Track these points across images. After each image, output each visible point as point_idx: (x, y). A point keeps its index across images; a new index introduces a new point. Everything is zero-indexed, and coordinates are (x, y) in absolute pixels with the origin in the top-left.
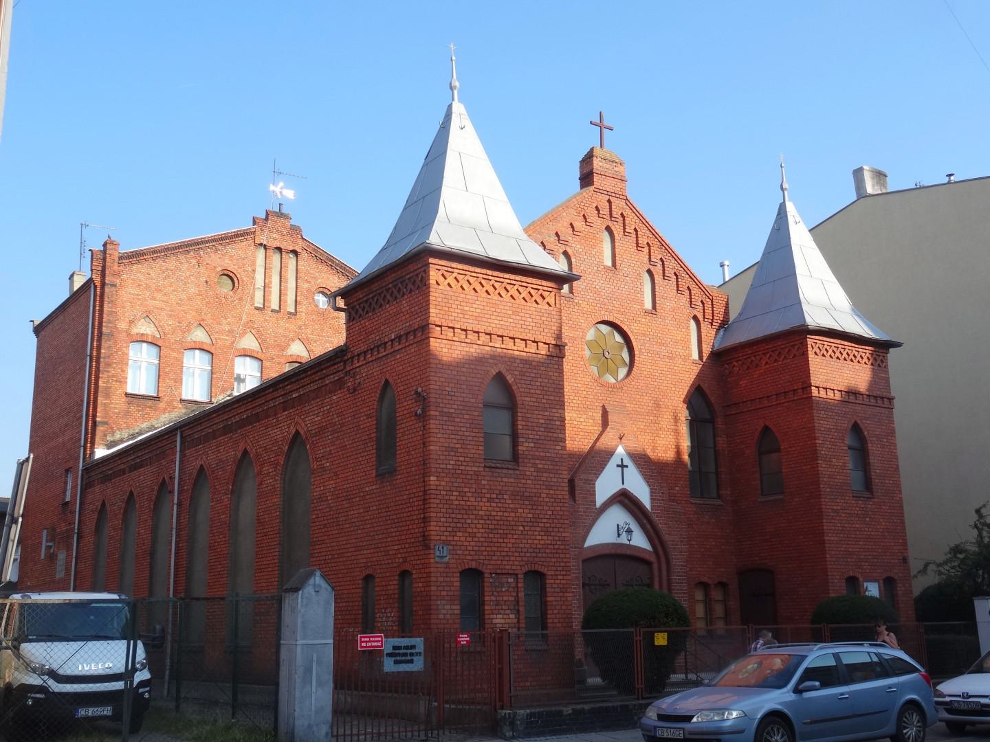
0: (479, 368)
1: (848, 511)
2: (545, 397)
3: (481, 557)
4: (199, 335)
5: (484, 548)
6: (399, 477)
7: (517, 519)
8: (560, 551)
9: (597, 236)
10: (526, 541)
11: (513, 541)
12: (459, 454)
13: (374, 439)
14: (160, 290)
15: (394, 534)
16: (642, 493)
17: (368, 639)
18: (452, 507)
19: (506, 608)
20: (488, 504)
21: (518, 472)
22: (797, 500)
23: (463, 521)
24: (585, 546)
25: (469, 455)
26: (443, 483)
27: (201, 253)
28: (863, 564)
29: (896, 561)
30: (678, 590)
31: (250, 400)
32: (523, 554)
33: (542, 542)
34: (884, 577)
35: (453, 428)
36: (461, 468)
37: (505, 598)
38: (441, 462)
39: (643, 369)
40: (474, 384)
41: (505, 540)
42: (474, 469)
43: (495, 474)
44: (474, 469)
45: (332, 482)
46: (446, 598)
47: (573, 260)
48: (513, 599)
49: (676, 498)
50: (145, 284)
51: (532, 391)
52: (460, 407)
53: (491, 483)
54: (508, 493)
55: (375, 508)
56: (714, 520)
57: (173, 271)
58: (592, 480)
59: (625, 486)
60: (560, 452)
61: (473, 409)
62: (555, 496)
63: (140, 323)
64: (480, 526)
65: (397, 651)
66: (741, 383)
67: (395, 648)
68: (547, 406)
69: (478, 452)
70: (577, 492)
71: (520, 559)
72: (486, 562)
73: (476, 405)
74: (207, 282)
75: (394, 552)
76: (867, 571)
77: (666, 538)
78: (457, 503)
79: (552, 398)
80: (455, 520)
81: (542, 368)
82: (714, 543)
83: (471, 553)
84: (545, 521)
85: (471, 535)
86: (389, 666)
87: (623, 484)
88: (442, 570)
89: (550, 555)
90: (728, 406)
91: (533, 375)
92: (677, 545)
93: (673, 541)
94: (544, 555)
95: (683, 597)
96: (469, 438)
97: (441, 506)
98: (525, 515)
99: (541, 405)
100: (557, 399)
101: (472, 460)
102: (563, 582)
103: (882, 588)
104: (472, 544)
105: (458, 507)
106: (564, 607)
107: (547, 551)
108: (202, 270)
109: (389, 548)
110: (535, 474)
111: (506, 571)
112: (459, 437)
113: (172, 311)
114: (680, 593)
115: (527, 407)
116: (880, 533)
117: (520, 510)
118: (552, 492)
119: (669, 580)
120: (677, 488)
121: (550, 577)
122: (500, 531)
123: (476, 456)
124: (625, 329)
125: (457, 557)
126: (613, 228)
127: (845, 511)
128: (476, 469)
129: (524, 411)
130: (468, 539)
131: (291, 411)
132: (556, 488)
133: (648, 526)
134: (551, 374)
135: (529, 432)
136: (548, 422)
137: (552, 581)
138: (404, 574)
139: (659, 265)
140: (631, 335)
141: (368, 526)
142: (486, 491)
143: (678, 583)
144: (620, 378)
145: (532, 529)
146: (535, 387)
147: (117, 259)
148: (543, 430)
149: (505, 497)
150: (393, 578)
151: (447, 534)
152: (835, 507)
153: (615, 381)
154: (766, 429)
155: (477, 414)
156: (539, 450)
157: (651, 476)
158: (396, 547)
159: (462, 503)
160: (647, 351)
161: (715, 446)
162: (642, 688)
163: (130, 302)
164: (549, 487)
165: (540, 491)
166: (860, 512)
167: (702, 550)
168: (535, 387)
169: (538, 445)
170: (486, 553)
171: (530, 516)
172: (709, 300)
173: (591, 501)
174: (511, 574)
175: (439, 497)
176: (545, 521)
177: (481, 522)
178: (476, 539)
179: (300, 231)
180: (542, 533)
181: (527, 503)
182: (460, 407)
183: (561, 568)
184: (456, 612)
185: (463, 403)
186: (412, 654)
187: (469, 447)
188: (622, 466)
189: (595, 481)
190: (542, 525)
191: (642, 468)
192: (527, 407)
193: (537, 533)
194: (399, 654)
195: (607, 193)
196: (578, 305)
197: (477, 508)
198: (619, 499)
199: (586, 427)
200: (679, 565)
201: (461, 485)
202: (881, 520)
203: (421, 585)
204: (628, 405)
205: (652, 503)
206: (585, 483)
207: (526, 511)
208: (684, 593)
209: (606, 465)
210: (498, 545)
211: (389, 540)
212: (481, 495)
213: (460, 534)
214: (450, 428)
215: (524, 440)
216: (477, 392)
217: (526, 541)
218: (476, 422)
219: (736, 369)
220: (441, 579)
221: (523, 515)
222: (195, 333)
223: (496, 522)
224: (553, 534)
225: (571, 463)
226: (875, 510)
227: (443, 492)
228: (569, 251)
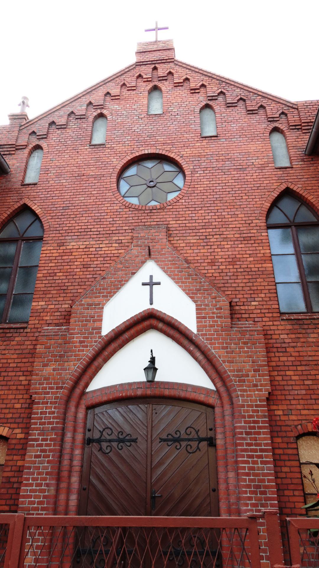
9: (141, 95)
30: (250, 445)
39: (196, 186)
49: (251, 316)
58: (99, 304)
77: (225, 367)
87: (151, 304)
92: (247, 376)
93: (238, 371)
95: (260, 457)
114: (256, 450)
120: (253, 303)
124: (172, 156)
133: (198, 354)
143: (247, 433)
157: (199, 290)
160: (202, 169)
167: (309, 382)
188: (151, 284)
191: (182, 282)
195: (152, 62)
200: (248, 406)
205: (198, 322)
206: (84, 309)
208: (262, 450)
228: (105, 112)
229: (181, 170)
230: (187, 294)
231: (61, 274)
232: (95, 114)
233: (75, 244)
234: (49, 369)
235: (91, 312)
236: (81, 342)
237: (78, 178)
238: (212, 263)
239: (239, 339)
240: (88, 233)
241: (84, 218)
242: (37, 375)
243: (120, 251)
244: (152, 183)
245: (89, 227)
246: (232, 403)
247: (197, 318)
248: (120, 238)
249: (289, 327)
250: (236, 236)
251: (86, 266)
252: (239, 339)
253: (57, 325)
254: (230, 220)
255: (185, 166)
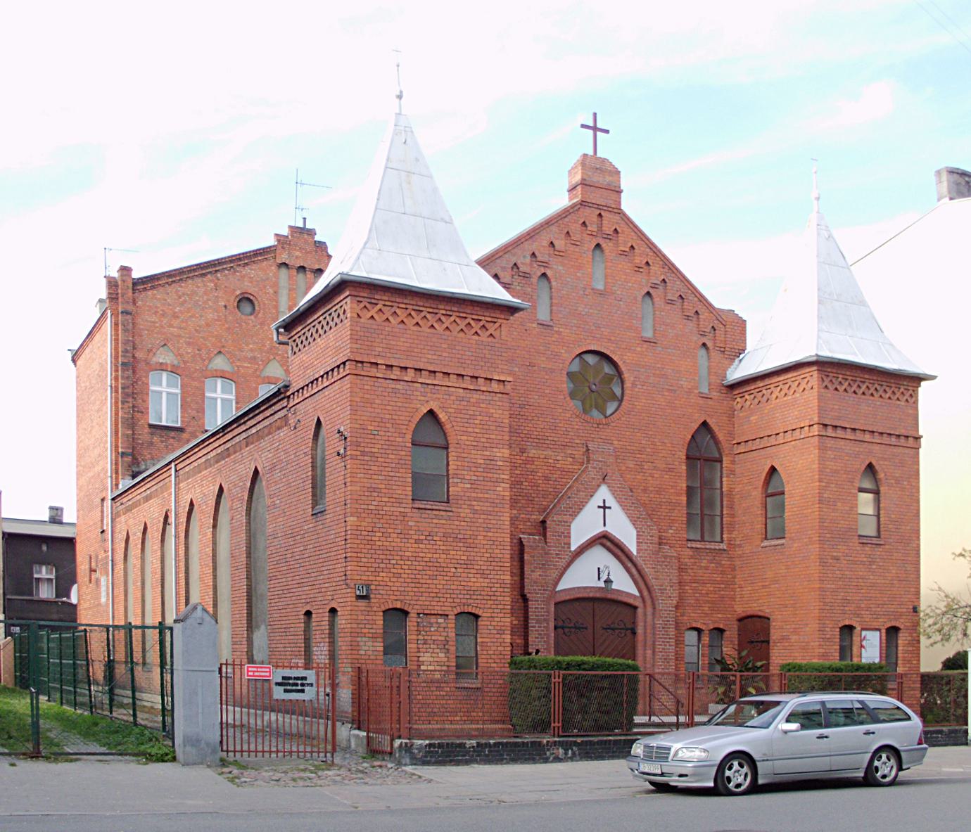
0: (407, 405)
1: (851, 558)
2: (485, 436)
3: (407, 597)
4: (220, 363)
5: (410, 589)
6: (328, 516)
7: (448, 561)
8: (499, 594)
10: (458, 583)
11: (444, 582)
12: (383, 495)
13: (310, 477)
14: (178, 317)
15: (325, 572)
16: (627, 535)
17: (255, 669)
18: (374, 547)
19: (435, 646)
20: (416, 545)
21: (451, 514)
22: (796, 545)
23: (387, 561)
24: (557, 590)
25: (394, 496)
26: (365, 524)
27: (219, 275)
28: (863, 612)
29: (905, 610)
31: (221, 435)
32: (455, 596)
33: (476, 584)
34: (889, 625)
35: (376, 468)
36: (385, 508)
37: (433, 638)
38: (362, 502)
39: (636, 403)
40: (401, 422)
41: (435, 582)
42: (400, 509)
43: (423, 516)
44: (400, 509)
45: (281, 519)
46: (367, 635)
47: (554, 283)
48: (443, 638)
50: (163, 311)
51: (470, 430)
52: (385, 447)
53: (419, 524)
54: (439, 534)
55: (311, 546)
56: (713, 565)
57: (190, 296)
59: (609, 529)
60: (502, 493)
61: (400, 448)
62: (495, 539)
63: (159, 352)
64: (406, 567)
65: (286, 681)
66: (752, 418)
67: (284, 678)
68: (488, 445)
69: (404, 492)
70: (548, 534)
71: (452, 600)
72: (412, 602)
73: (403, 444)
74: (225, 306)
75: (325, 590)
76: (868, 620)
77: (653, 582)
78: (380, 543)
79: (493, 437)
80: (377, 561)
81: (482, 405)
82: (712, 589)
83: (396, 593)
84: (480, 563)
85: (396, 575)
86: (279, 693)
87: (605, 525)
88: (363, 608)
89: (486, 597)
90: (739, 443)
91: (471, 413)
93: (661, 586)
94: (479, 597)
96: (395, 479)
97: (363, 546)
98: (458, 557)
99: (479, 444)
100: (499, 437)
101: (398, 500)
102: (499, 624)
103: (884, 638)
104: (396, 584)
105: (381, 548)
106: (499, 648)
107: (482, 593)
108: (221, 294)
109: (321, 586)
110: (471, 515)
111: (436, 612)
112: (383, 478)
113: (190, 338)
115: (463, 446)
116: (887, 582)
117: (452, 552)
118: (490, 534)
119: (654, 628)
120: (671, 531)
121: (485, 619)
122: (428, 572)
123: (401, 497)
124: (615, 359)
125: (380, 596)
126: (604, 245)
127: (847, 558)
128: (402, 510)
129: (459, 450)
130: (393, 579)
131: (252, 446)
132: (495, 530)
133: (634, 571)
134: (492, 411)
135: (466, 473)
136: (488, 462)
137: (489, 623)
138: (333, 611)
139: (661, 287)
140: (623, 368)
141: (307, 563)
142: (413, 532)
144: (609, 412)
145: (466, 571)
146: (474, 426)
147: (131, 285)
148: (482, 470)
149: (435, 538)
150: (324, 615)
151: (369, 573)
152: (835, 554)
153: (602, 417)
154: (773, 470)
155: (404, 453)
156: (477, 491)
158: (327, 585)
159: (385, 543)
161: (721, 488)
162: (559, 727)
163: (148, 330)
164: (489, 529)
165: (476, 533)
166: (865, 559)
167: (697, 595)
168: (474, 426)
169: (475, 486)
170: (412, 594)
171: (465, 558)
172: (722, 326)
173: (565, 544)
174: (441, 615)
175: (359, 537)
176: (482, 563)
177: (407, 562)
178: (403, 580)
179: (326, 248)
180: (479, 576)
181: (461, 545)
182: (385, 447)
183: (499, 611)
184: (378, 649)
185: (387, 443)
186: (302, 685)
187: (394, 487)
188: (604, 507)
189: (571, 523)
190: (479, 567)
192: (463, 446)
193: (472, 575)
194: (289, 684)
196: (559, 333)
197: (403, 549)
198: (597, 542)
199: (565, 466)
201: (385, 526)
202: (891, 568)
203: (344, 622)
204: (616, 442)
205: (638, 546)
207: (461, 553)
209: (584, 506)
210: (427, 586)
211: (321, 577)
212: (407, 536)
213: (384, 574)
214: (373, 468)
215: (459, 480)
216: (404, 432)
217: (458, 583)
218: (403, 462)
219: (748, 403)
220: (363, 617)
221: (455, 557)
222: (216, 362)
223: (424, 564)
224: (489, 576)
225: (545, 503)
226: (885, 557)
227: (363, 533)
228: (549, 273)
229: (619, 373)
230: (631, 521)
231: (527, 484)
232: (540, 274)
233: (535, 452)
234: (536, 575)
235: (562, 529)
236: (557, 554)
237: (530, 368)
238: (645, 490)
239: (663, 562)
240: (547, 442)
241: (540, 423)
242: (528, 578)
243: (575, 467)
244: (594, 387)
245: (547, 434)
246: (654, 608)
247: (638, 542)
248: (573, 452)
249: (691, 553)
250: (665, 466)
251: (547, 479)
252: (663, 562)
253: (530, 534)
254: (660, 448)
255: (626, 375)
